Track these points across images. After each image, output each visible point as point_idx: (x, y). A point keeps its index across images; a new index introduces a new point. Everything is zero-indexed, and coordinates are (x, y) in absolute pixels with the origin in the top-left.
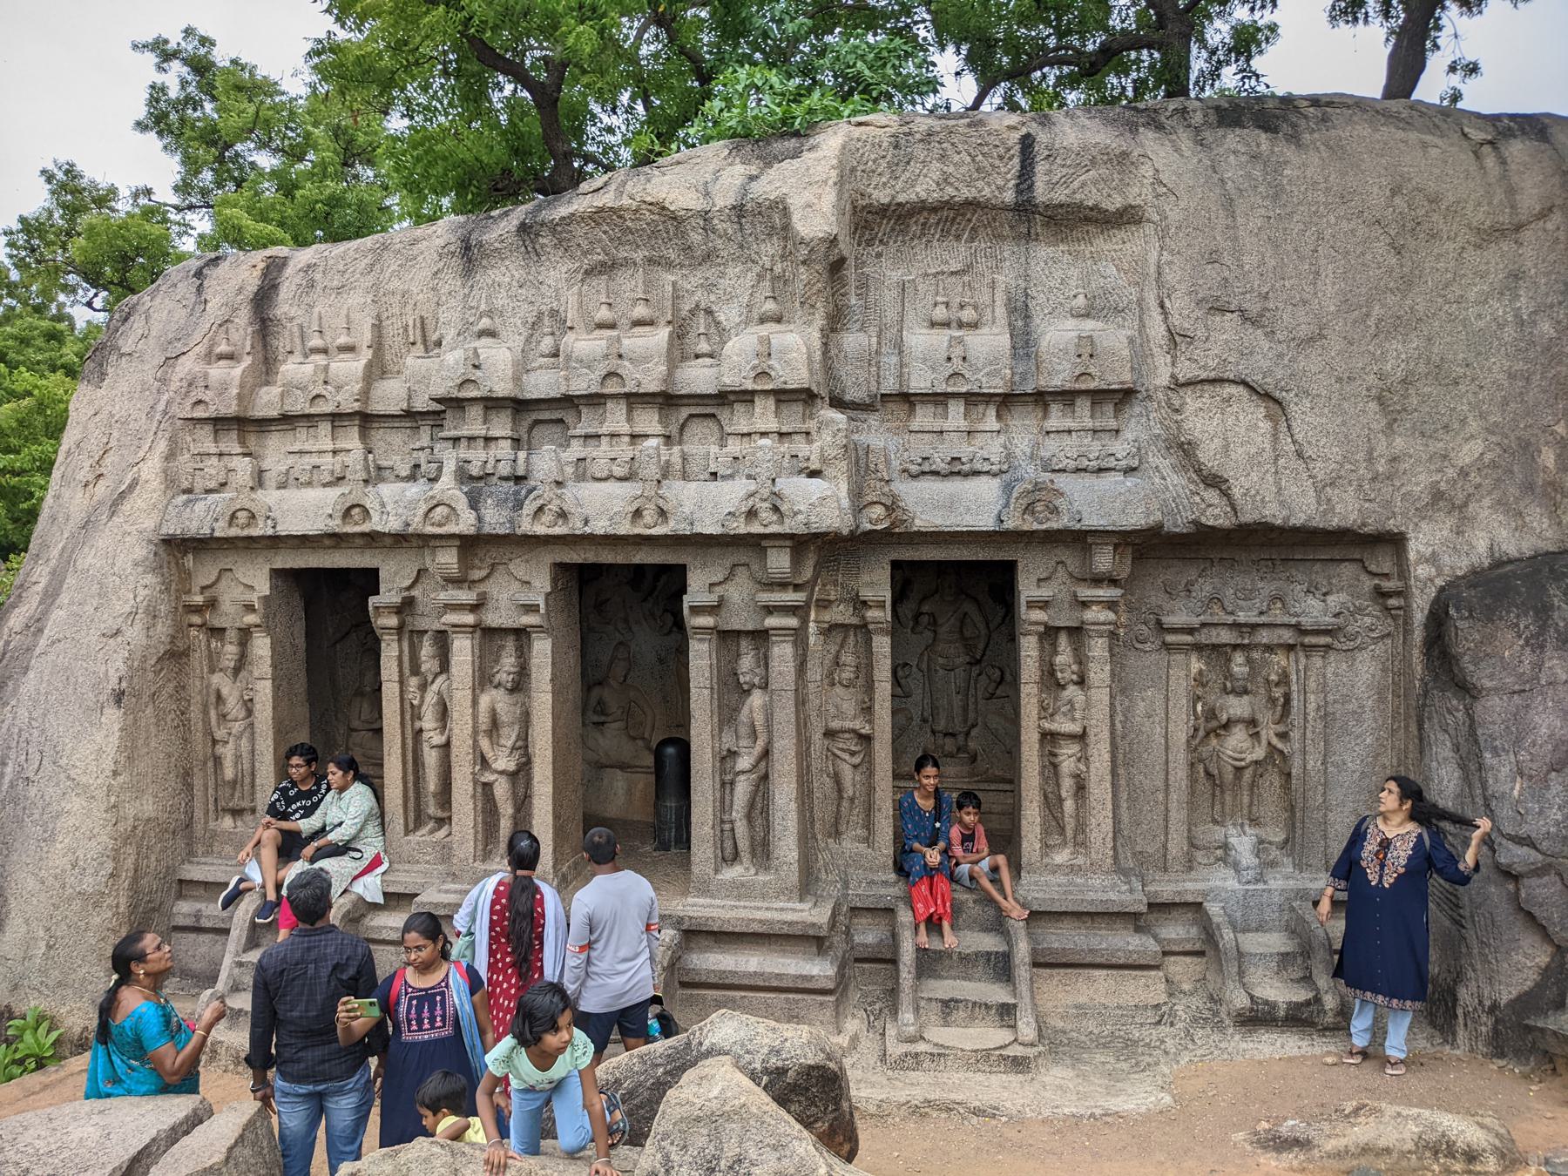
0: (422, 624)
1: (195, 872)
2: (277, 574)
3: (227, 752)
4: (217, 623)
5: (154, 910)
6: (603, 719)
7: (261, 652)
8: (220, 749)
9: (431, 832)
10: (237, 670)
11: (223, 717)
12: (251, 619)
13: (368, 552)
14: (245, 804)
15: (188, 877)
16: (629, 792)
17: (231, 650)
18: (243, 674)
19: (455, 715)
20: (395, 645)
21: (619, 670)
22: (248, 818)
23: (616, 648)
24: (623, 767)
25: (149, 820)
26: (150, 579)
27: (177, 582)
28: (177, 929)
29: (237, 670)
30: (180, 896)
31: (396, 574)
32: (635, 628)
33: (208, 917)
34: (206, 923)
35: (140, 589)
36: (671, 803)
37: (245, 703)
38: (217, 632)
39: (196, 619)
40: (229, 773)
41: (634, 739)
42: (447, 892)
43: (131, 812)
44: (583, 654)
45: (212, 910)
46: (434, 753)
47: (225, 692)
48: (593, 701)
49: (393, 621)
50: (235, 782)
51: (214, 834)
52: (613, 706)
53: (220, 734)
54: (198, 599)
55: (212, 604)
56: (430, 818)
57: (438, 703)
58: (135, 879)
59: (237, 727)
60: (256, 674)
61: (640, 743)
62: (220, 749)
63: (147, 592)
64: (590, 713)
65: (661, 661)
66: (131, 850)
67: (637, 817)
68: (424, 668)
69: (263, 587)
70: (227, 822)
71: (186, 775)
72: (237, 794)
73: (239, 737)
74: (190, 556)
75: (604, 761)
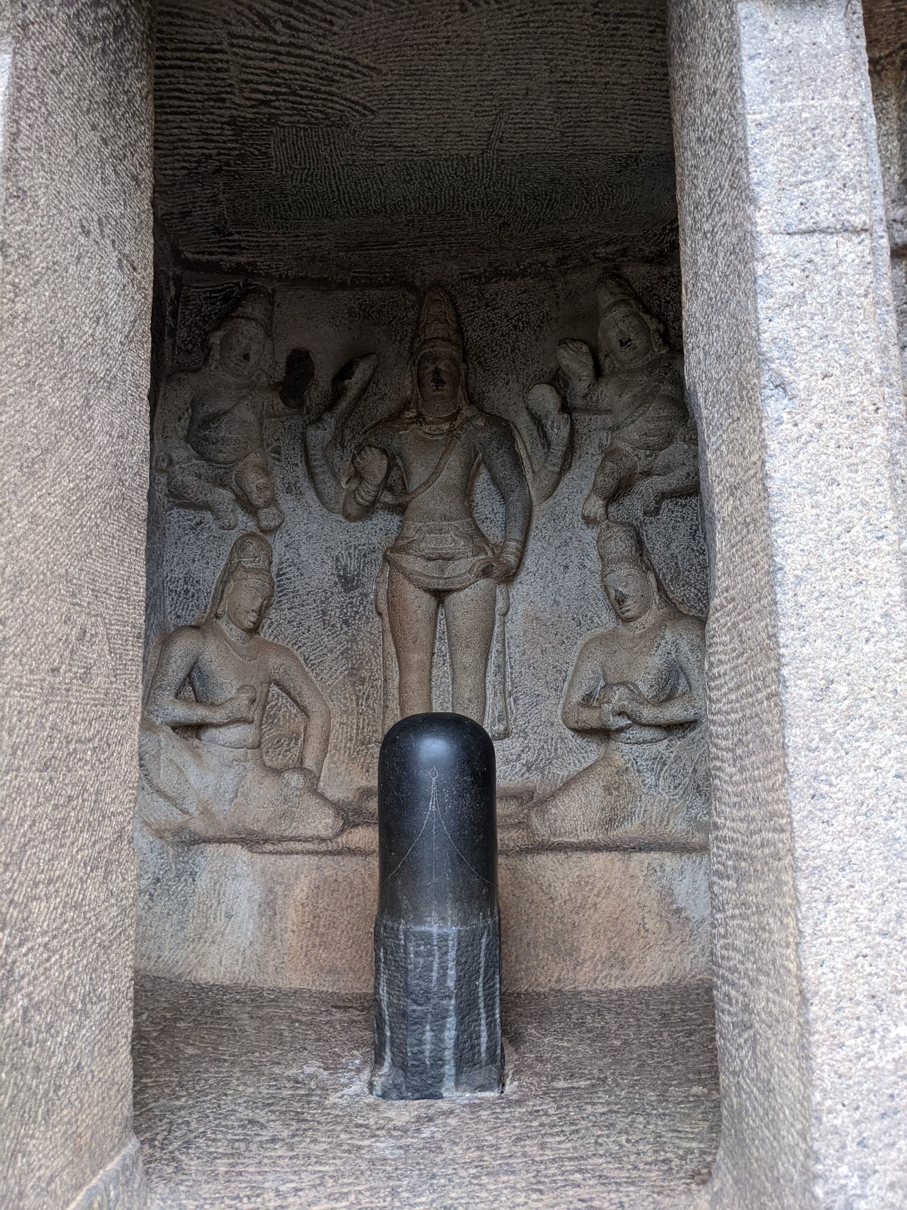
6: (198, 713)
16: (269, 908)
21: (246, 596)
23: (239, 547)
24: (251, 840)
32: (287, 502)
36: (439, 927)
41: (278, 772)
44: (154, 558)
48: (176, 668)
52: (229, 684)
61: (295, 779)
64: (166, 698)
65: (348, 582)
67: (293, 980)
75: (198, 825)
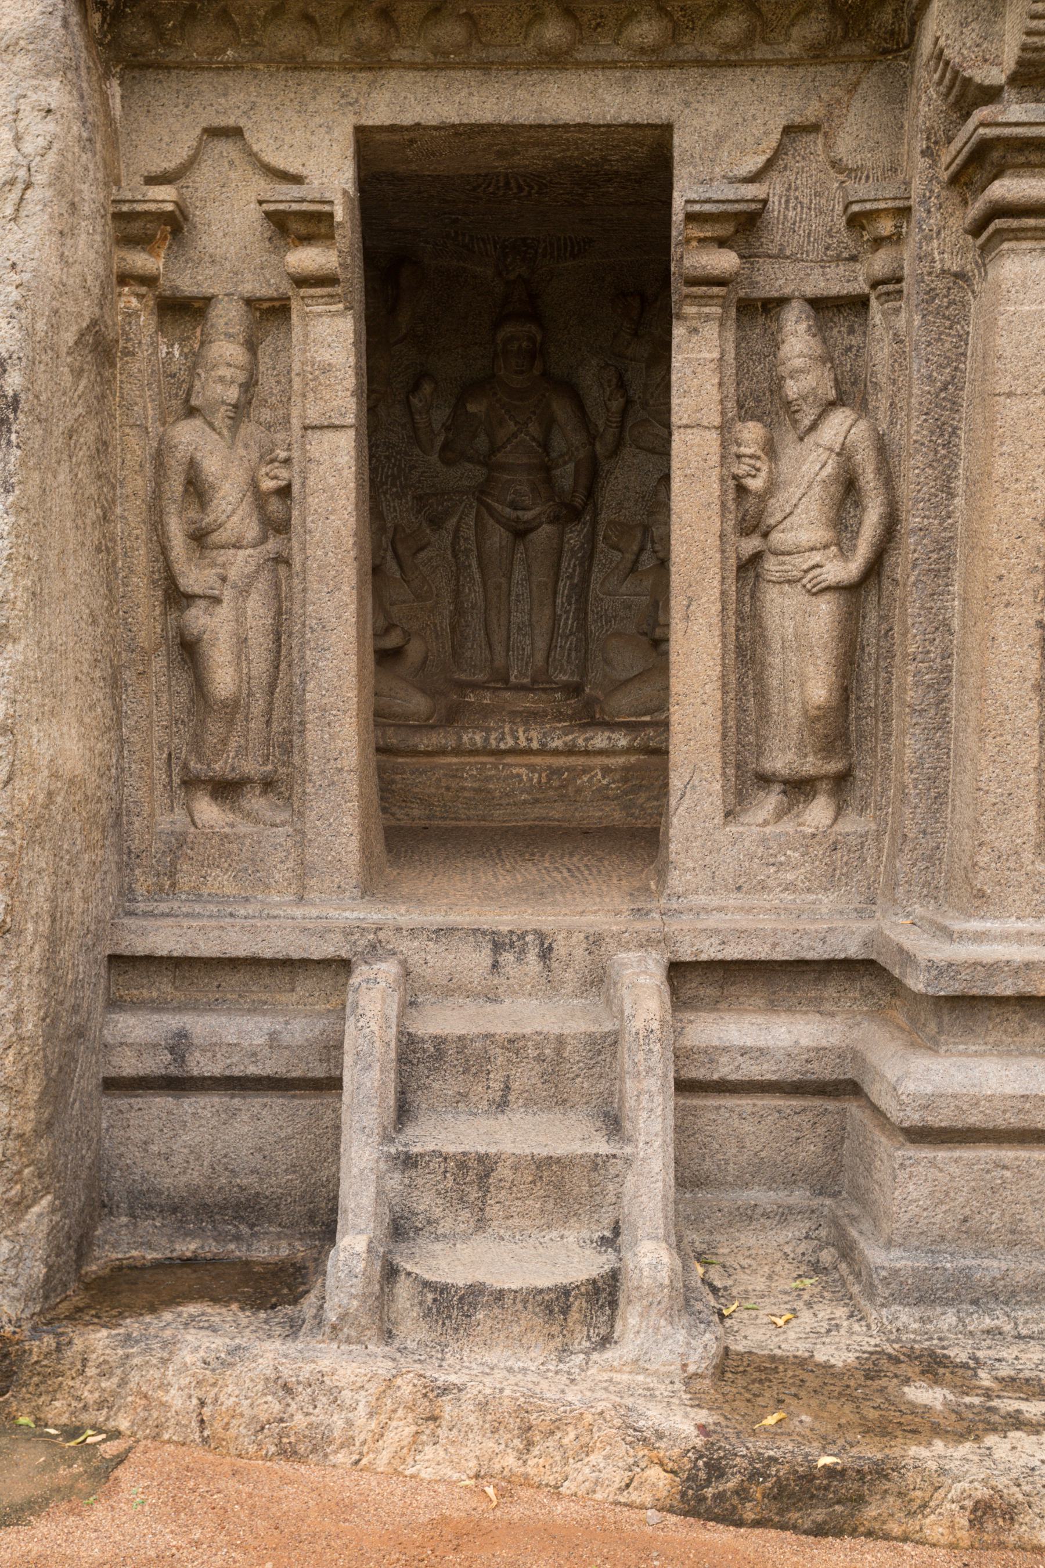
0: (775, 279)
1: (164, 939)
2: (368, 143)
3: (214, 626)
4: (187, 283)
5: (80, 1033)
7: (325, 356)
8: (197, 618)
9: (780, 814)
10: (240, 411)
11: (200, 538)
12: (308, 258)
13: (643, 82)
14: (251, 767)
15: (141, 947)
17: (227, 352)
18: (248, 429)
19: (1001, 467)
20: (710, 331)
22: (255, 802)
25: (72, 782)
26: (55, 93)
27: (107, 137)
28: (113, 1085)
29: (240, 411)
30: (114, 1004)
31: (720, 138)
33: (211, 1048)
34: (201, 1065)
35: (30, 119)
37: (260, 499)
38: (182, 311)
39: (141, 261)
40: (223, 680)
42: (979, 937)
43: (43, 751)
45: (235, 1033)
46: (826, 608)
47: (211, 466)
49: (725, 261)
50: (233, 707)
51: (178, 845)
53: (193, 578)
54: (164, 196)
55: (175, 225)
56: (764, 780)
57: (835, 478)
58: (54, 942)
59: (241, 563)
60: (313, 416)
62: (197, 618)
63: (50, 126)
66: (40, 858)
68: (792, 389)
69: (331, 177)
70: (209, 811)
71: (115, 683)
72: (233, 744)
73: (244, 592)
74: (115, 89)
